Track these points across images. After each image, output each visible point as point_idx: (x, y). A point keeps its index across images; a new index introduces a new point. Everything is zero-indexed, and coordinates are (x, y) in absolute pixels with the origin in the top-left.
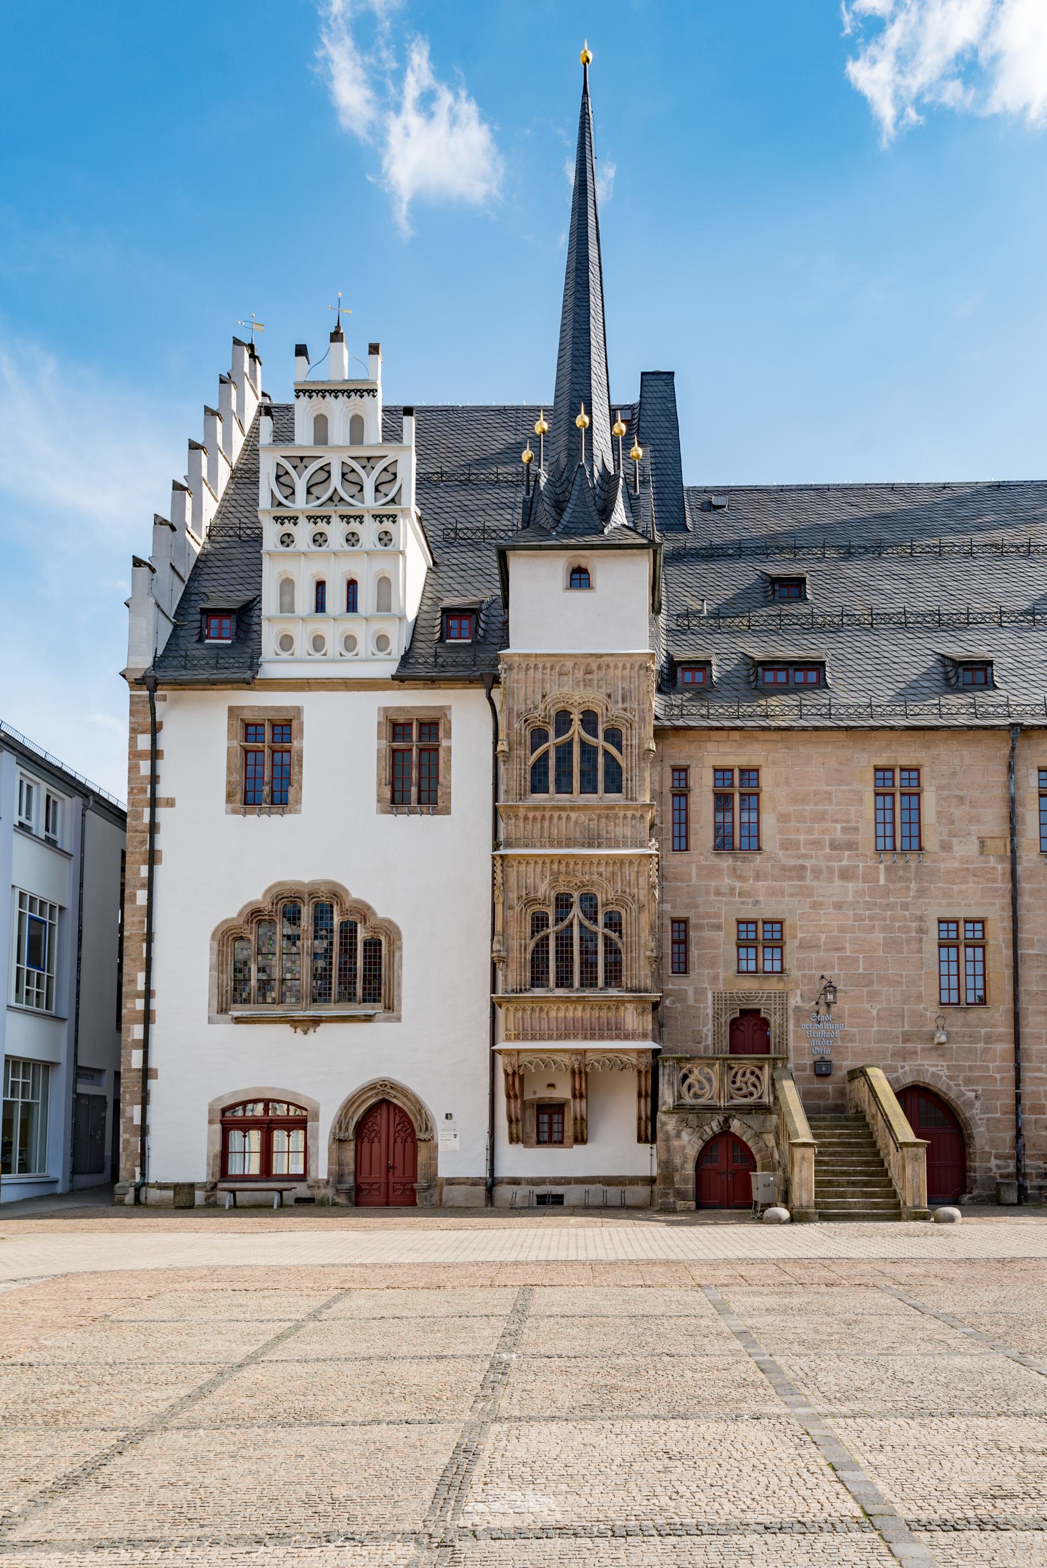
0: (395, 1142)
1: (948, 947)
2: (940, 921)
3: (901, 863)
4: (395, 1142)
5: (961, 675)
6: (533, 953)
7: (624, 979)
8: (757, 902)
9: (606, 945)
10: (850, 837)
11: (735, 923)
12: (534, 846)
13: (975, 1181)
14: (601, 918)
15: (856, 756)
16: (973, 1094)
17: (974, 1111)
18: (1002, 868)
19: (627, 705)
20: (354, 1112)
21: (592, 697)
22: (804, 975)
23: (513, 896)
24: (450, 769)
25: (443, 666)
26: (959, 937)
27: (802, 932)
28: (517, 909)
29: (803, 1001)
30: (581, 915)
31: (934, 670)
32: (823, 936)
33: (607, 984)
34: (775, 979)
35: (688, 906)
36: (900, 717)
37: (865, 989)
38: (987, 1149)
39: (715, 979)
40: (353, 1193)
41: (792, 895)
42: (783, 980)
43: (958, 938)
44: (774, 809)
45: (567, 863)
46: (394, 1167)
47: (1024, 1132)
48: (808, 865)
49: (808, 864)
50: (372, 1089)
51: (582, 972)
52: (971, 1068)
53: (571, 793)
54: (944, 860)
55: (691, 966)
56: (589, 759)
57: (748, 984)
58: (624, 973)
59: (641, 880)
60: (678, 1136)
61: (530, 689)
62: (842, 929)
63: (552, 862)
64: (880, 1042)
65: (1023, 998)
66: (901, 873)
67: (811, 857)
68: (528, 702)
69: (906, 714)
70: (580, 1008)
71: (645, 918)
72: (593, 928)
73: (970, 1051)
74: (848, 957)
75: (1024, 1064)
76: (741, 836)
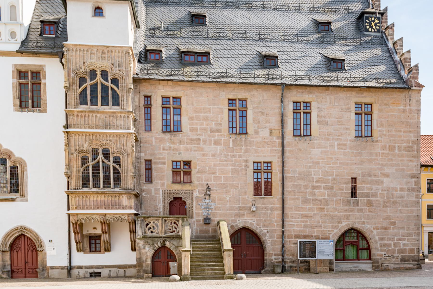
0: (28, 252)
1: (257, 173)
2: (254, 163)
3: (239, 138)
4: (28, 252)
5: (265, 61)
6: (83, 173)
7: (122, 184)
8: (180, 153)
9: (114, 170)
10: (218, 127)
11: (171, 162)
12: (81, 128)
13: (266, 265)
14: (111, 159)
15: (221, 93)
16: (266, 231)
17: (266, 237)
18: (278, 141)
19: (120, 69)
20: (9, 239)
21: (106, 65)
22: (200, 184)
23: (73, 149)
24: (46, 93)
25: (40, 47)
26: (261, 168)
27: (199, 166)
28: (75, 154)
29: (199, 194)
30: (103, 158)
31: (255, 59)
32: (207, 168)
33: (115, 187)
34: (188, 185)
35: (151, 154)
36: (238, 78)
37: (224, 189)
38: (271, 252)
39: (163, 185)
40: (10, 273)
41: (195, 151)
42: (191, 186)
43: (261, 169)
44: (187, 115)
45: (96, 135)
46: (28, 262)
47: (285, 245)
48: (201, 138)
49: (201, 138)
50: (16, 230)
51: (104, 182)
52: (265, 221)
53: (98, 105)
54: (256, 138)
55: (153, 179)
56: (105, 91)
57: (177, 187)
58: (122, 182)
59: (128, 143)
60: (144, 248)
61: (78, 60)
62: (215, 165)
63: (89, 135)
64: (230, 210)
65: (286, 193)
66: (238, 143)
67: (202, 135)
68: (77, 65)
69: (241, 77)
70: (103, 196)
71: (130, 160)
72: (108, 163)
73: (265, 214)
74: (217, 177)
75: (286, 219)
76: (174, 126)
